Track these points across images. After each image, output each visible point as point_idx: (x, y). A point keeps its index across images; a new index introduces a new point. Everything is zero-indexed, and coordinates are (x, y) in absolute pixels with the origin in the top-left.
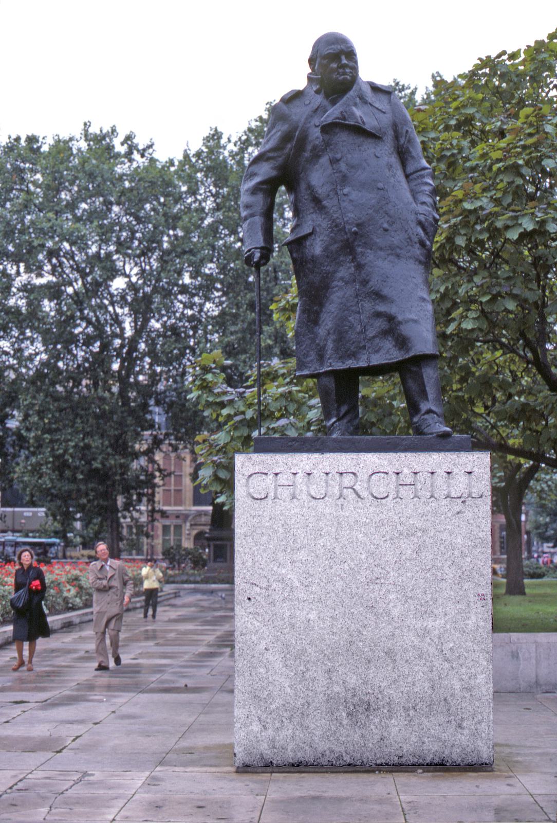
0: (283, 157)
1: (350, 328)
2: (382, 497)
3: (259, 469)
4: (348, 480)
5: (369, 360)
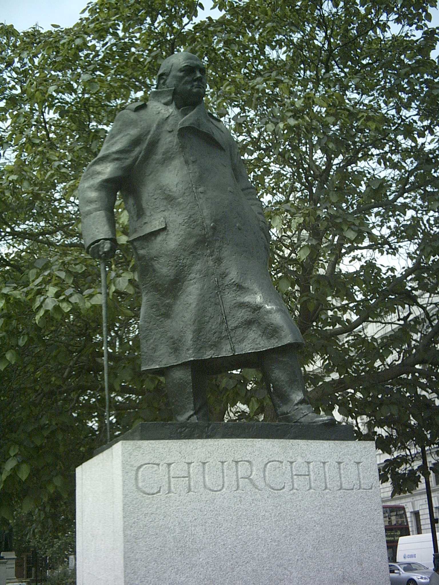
0: (131, 159)
1: (211, 318)
2: (279, 488)
5: (233, 349)
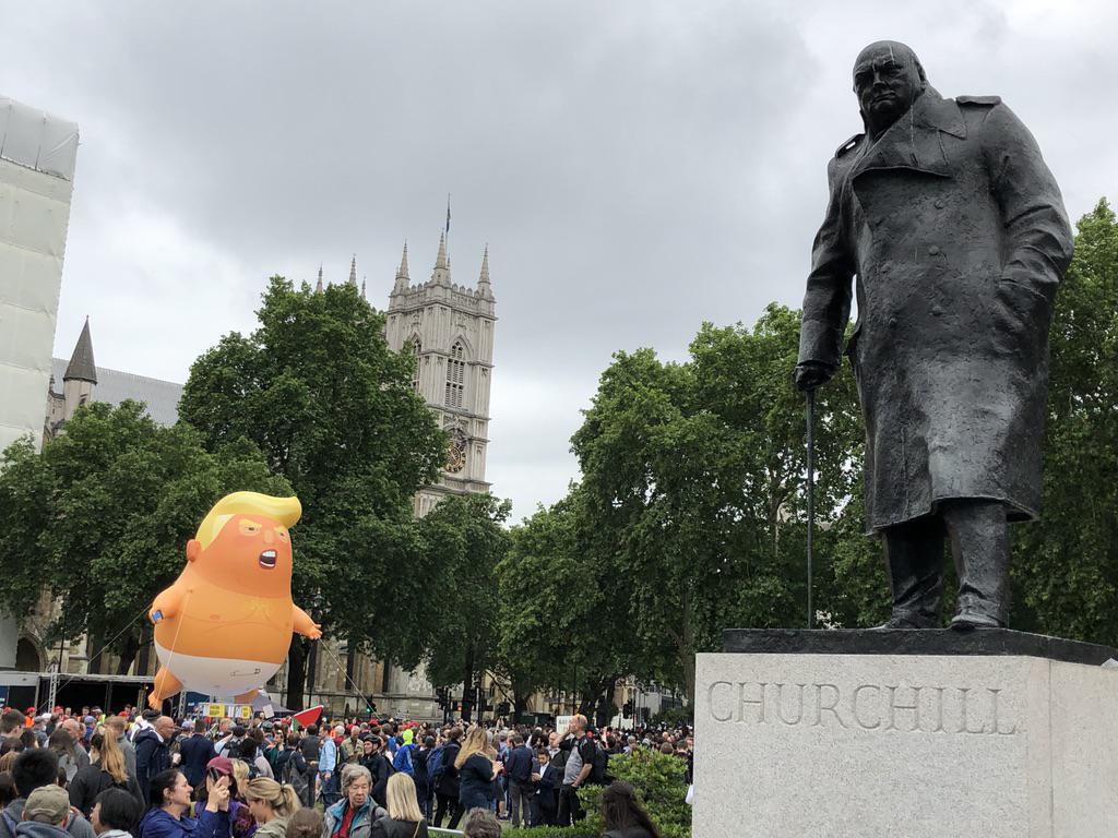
1: (893, 465)
3: (723, 677)
4: (828, 696)
